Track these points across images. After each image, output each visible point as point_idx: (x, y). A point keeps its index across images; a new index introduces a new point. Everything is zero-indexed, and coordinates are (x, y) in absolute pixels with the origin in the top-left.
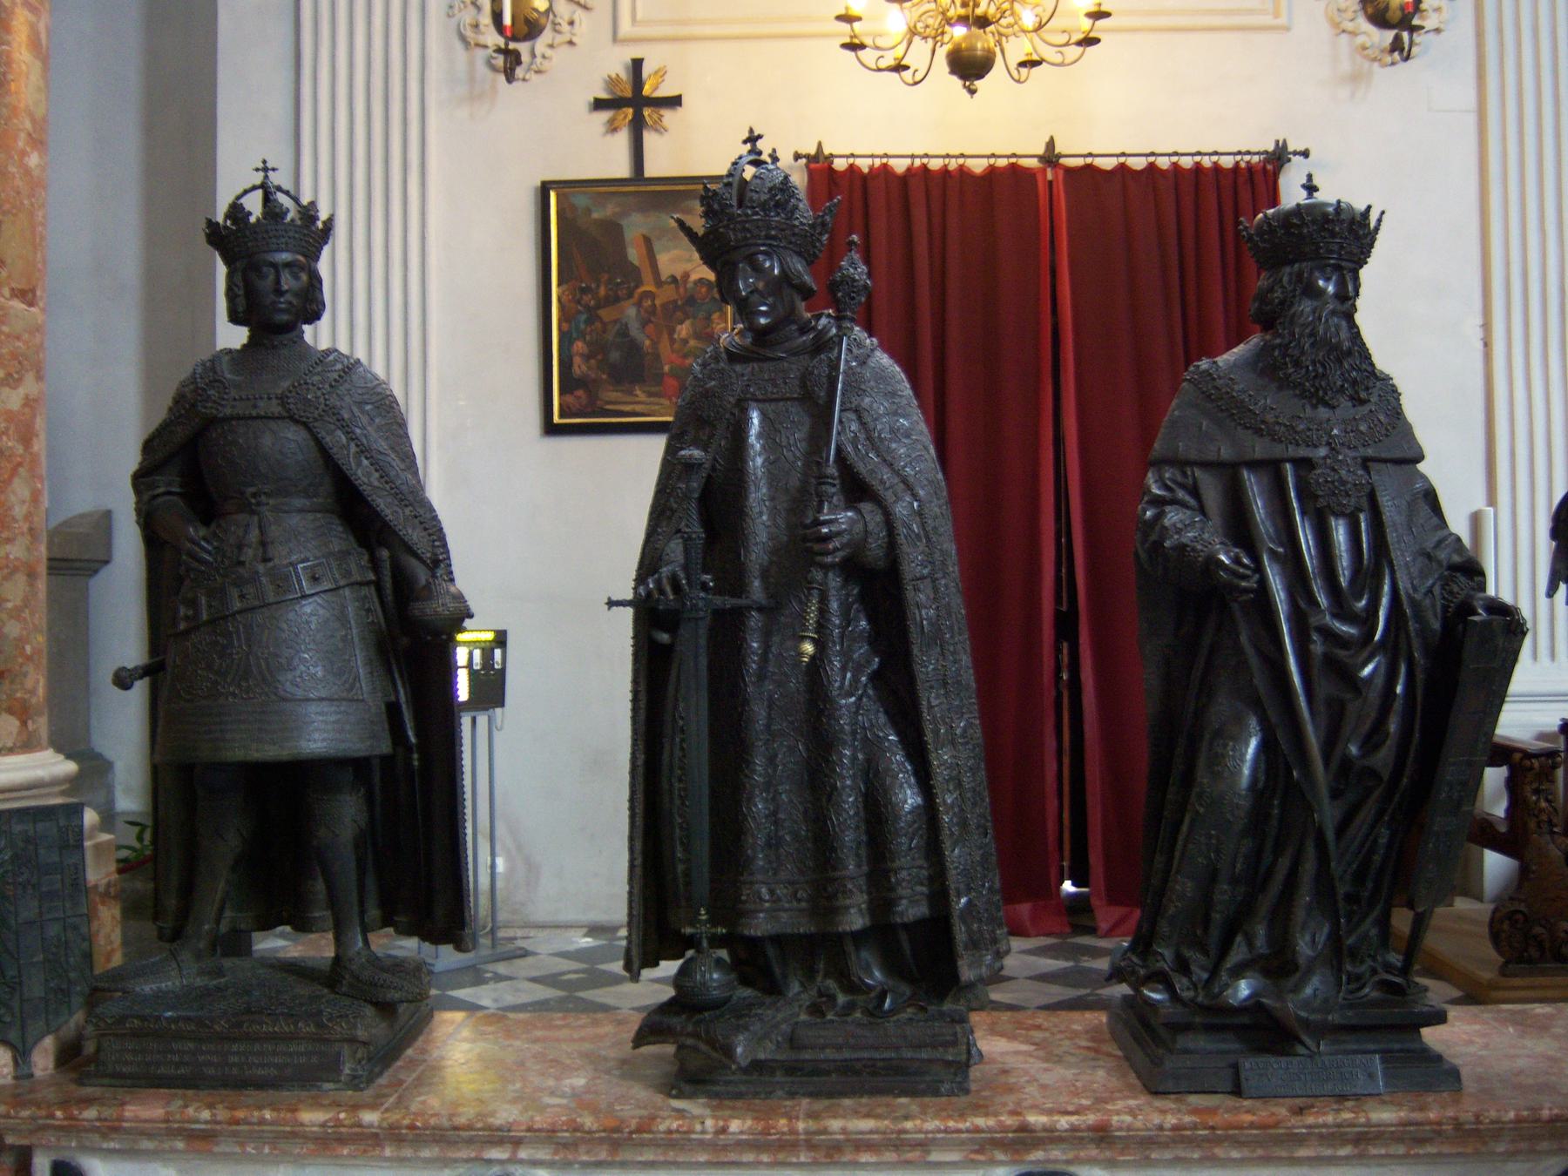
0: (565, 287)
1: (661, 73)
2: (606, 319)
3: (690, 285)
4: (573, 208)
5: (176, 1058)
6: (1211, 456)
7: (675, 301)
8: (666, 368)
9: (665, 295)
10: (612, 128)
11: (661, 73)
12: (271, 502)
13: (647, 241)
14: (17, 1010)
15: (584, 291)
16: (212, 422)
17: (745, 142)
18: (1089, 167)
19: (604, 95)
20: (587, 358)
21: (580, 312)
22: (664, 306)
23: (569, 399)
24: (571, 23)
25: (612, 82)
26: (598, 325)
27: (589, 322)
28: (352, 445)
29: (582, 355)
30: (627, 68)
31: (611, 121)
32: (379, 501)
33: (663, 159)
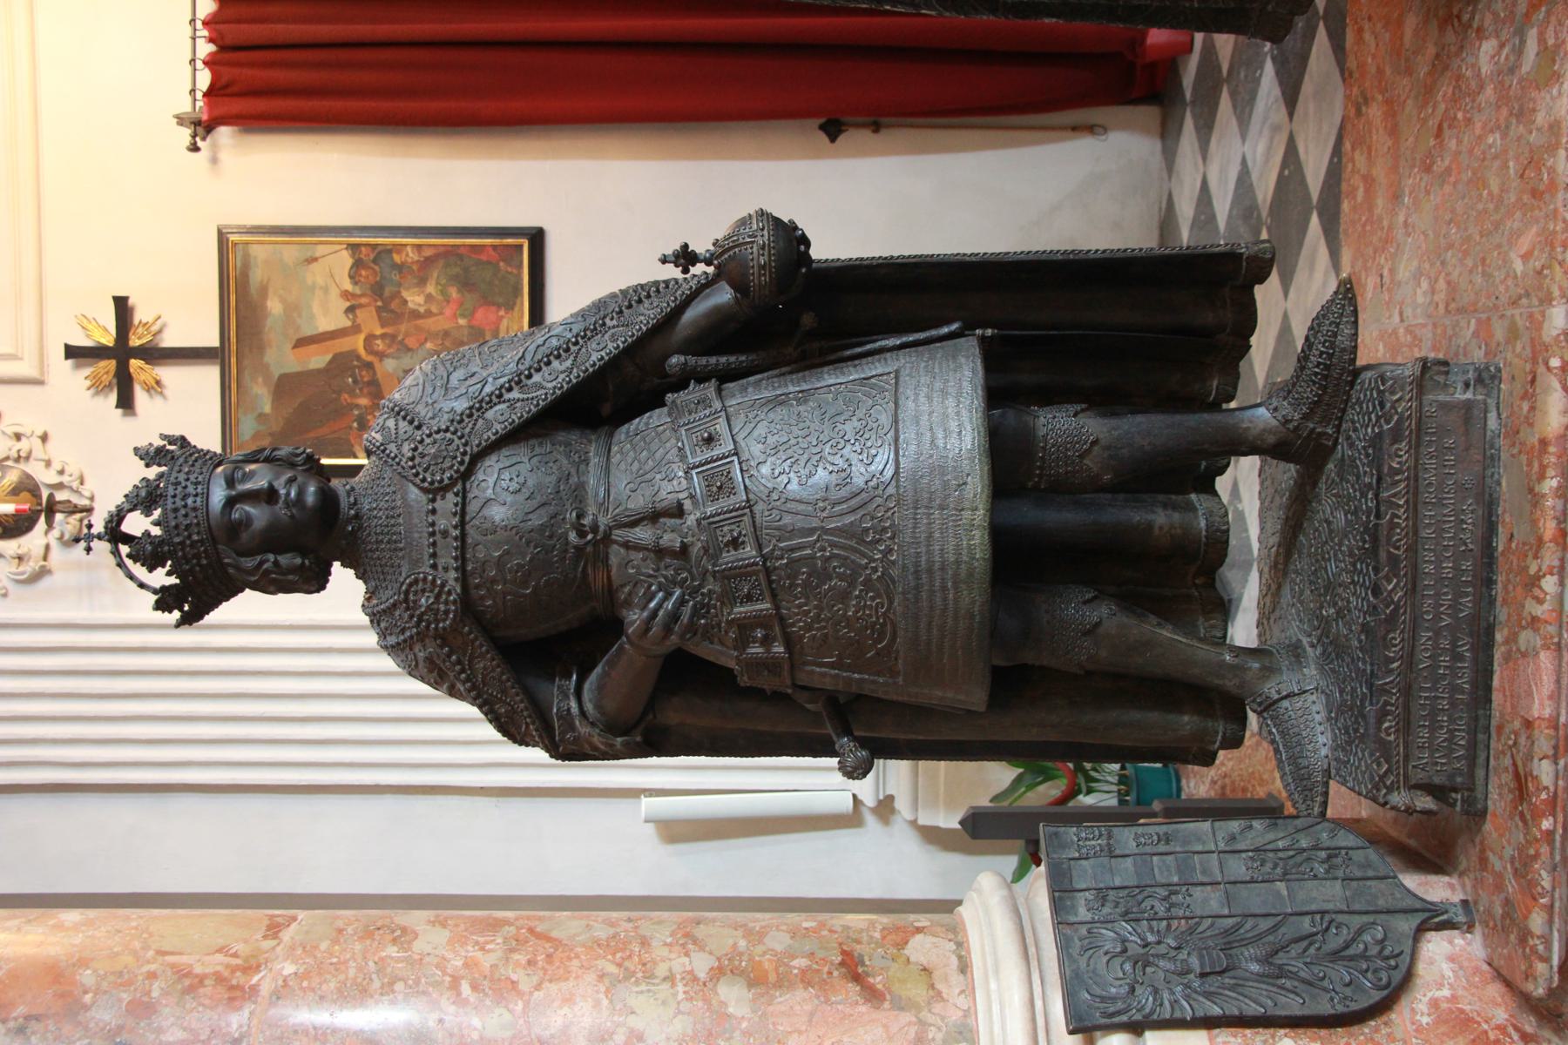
1: (84, 323)
3: (358, 291)
5: (1445, 659)
7: (378, 310)
8: (462, 322)
9: (370, 322)
10: (156, 387)
11: (84, 323)
12: (591, 510)
13: (301, 343)
14: (1366, 919)
16: (467, 604)
22: (383, 326)
24: (18, 437)
25: (98, 388)
28: (507, 396)
30: (78, 367)
31: (148, 389)
32: (595, 357)
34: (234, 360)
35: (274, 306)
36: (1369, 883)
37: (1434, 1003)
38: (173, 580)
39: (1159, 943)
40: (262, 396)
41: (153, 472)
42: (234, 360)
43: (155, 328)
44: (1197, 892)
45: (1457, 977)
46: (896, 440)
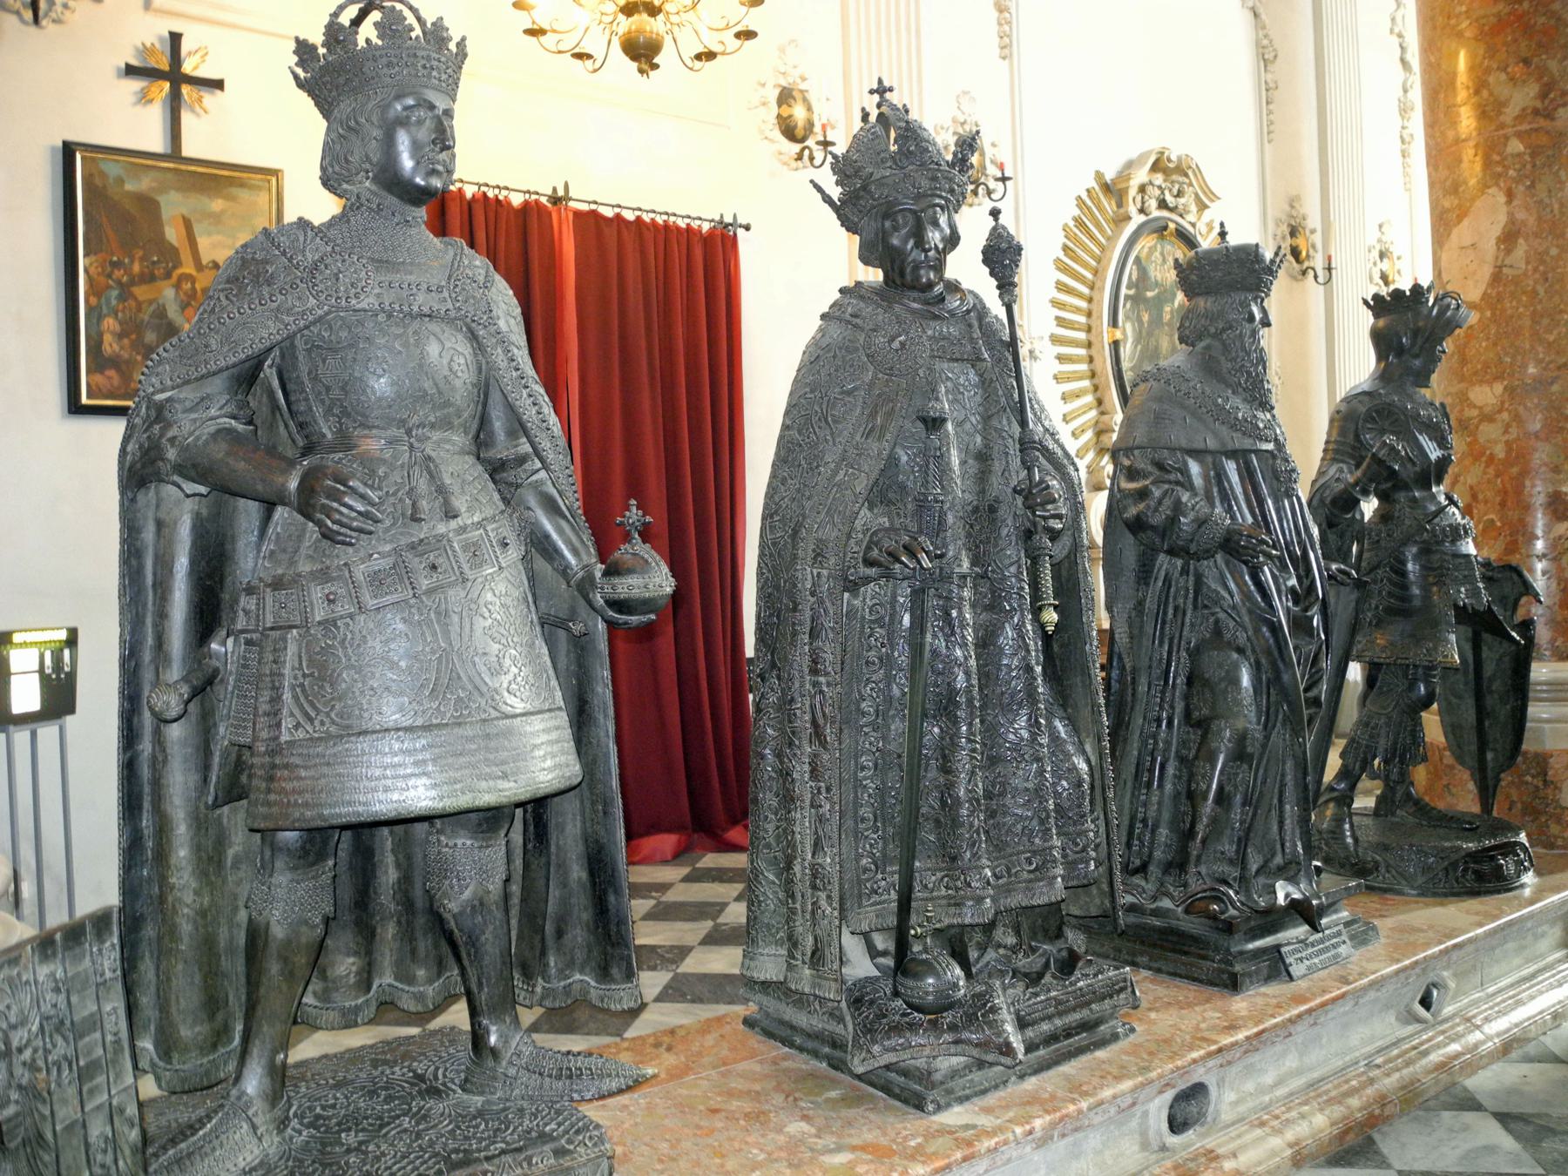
0: (93, 258)
2: (141, 298)
4: (103, 175)
6: (1199, 445)
10: (144, 98)
13: (188, 224)
15: (115, 265)
17: (872, 92)
18: (594, 212)
19: (134, 62)
20: (120, 336)
21: (109, 287)
23: (98, 378)
25: (145, 51)
26: (132, 303)
27: (122, 298)
29: (114, 333)
33: (204, 137)
34: (171, 165)
35: (217, 205)
38: (361, 43)
40: (144, 184)
41: (452, 46)
42: (171, 165)
43: (197, 108)
46: (532, 714)
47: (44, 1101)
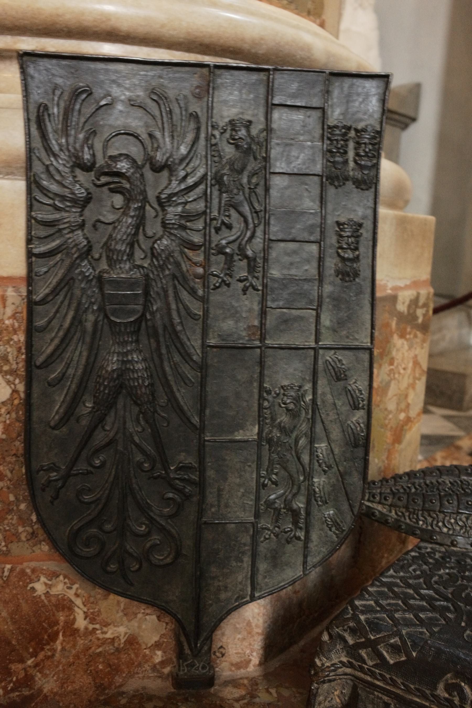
36: (247, 560)
37: (65, 605)
39: (164, 225)
44: (249, 304)
45: (104, 642)
47: (193, 292)
